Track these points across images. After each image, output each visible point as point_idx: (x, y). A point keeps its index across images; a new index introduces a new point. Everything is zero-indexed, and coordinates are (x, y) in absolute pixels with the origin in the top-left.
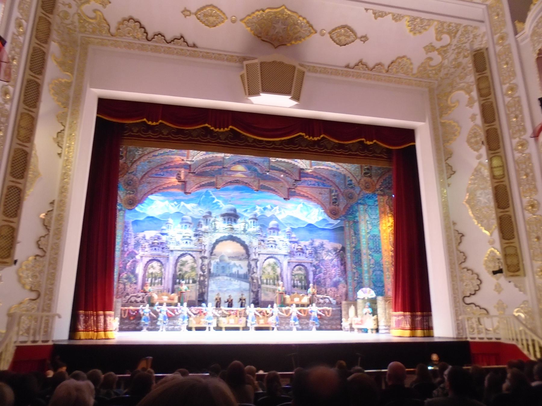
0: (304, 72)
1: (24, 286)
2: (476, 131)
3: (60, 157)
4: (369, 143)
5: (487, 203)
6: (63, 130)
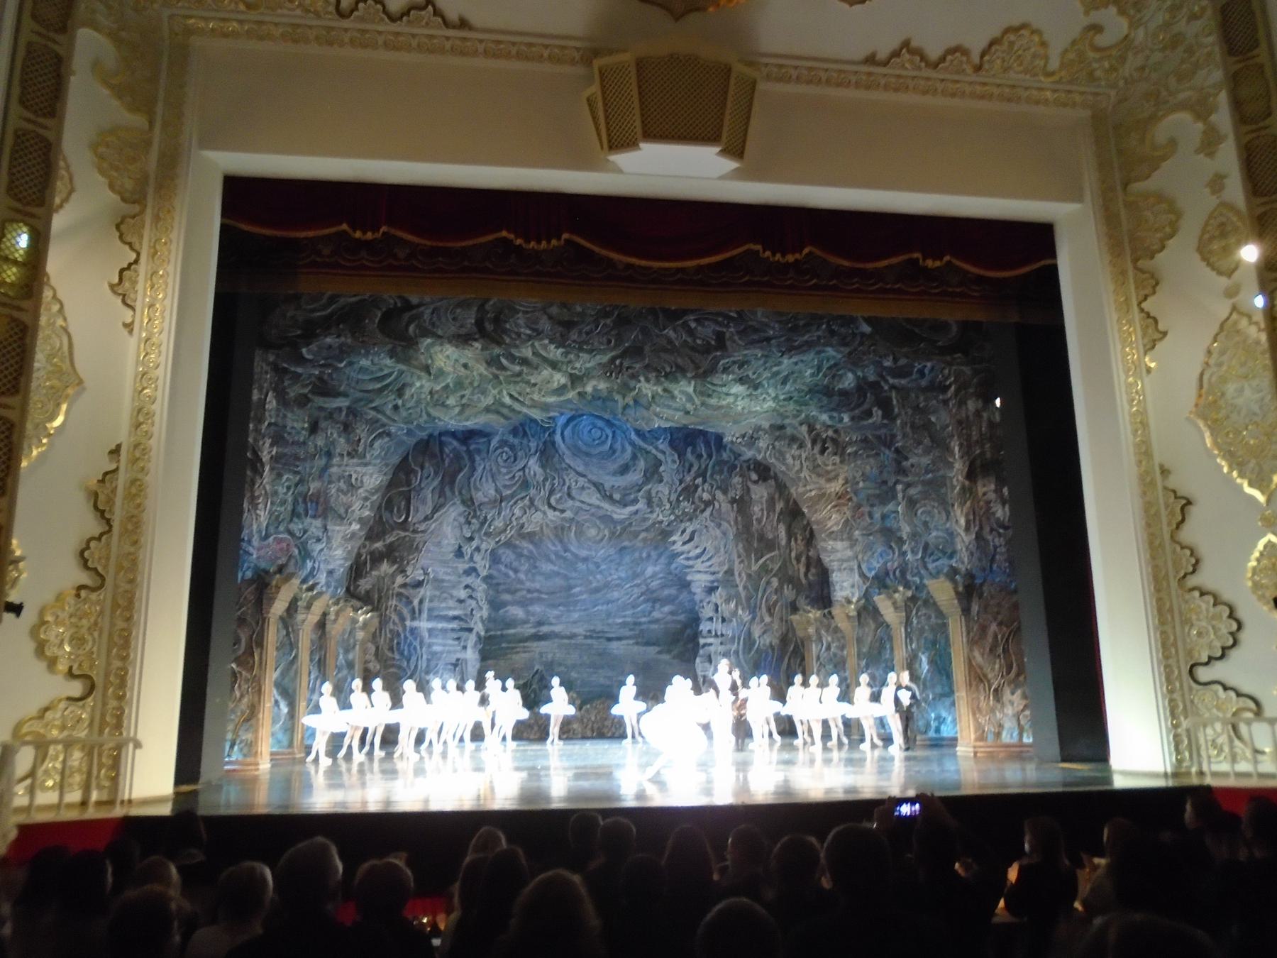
0: (754, 84)
1: (52, 663)
2: (1224, 220)
3: (131, 332)
4: (930, 263)
5: (1255, 414)
6: (136, 262)
